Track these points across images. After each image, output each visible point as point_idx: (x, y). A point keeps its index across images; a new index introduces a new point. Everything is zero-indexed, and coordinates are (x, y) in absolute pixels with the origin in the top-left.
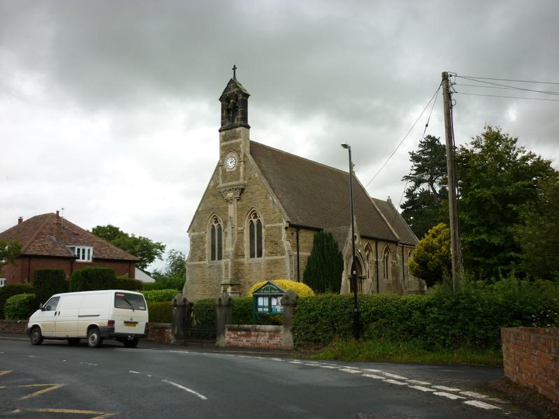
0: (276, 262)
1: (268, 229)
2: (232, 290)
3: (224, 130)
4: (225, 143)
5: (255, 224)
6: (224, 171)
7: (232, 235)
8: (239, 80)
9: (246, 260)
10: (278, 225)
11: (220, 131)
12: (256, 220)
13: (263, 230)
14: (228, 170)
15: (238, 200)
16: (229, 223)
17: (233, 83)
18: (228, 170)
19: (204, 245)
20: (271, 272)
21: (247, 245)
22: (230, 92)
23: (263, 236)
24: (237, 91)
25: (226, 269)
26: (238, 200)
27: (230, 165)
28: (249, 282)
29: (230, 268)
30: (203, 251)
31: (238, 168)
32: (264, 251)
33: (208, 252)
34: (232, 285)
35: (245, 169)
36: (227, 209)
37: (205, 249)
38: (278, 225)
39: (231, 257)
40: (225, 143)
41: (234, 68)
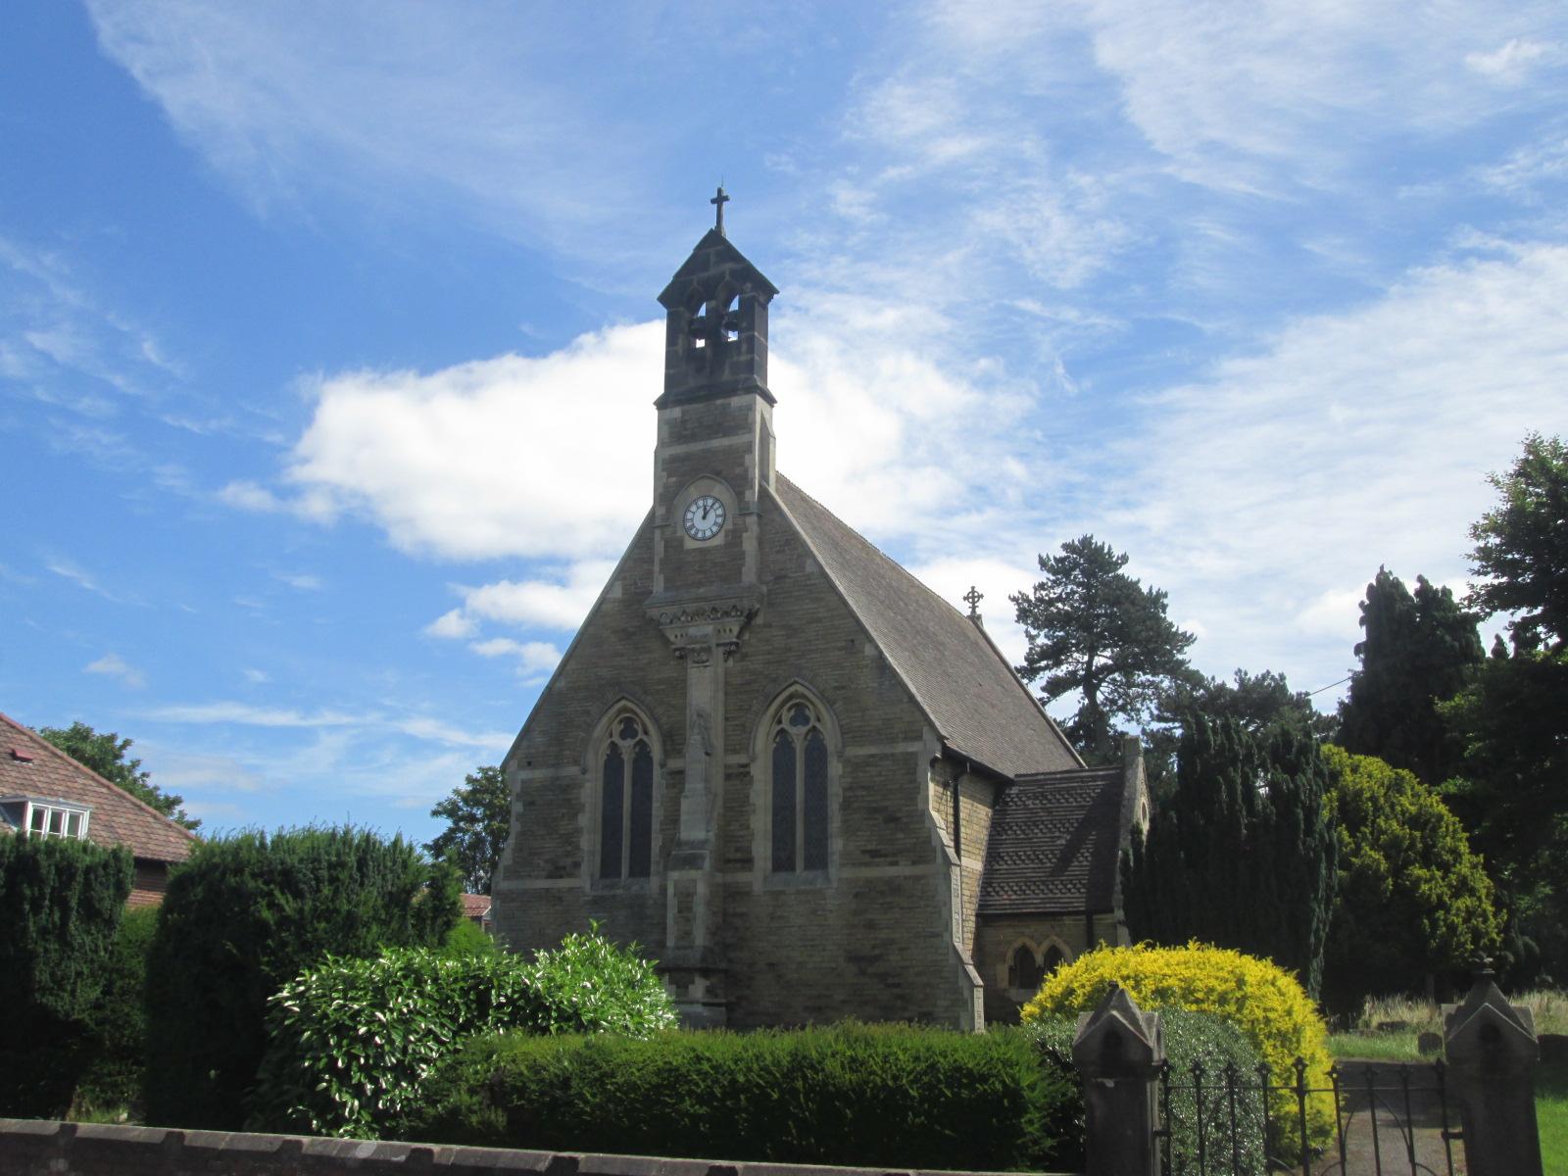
0: (893, 887)
1: (855, 766)
2: (709, 991)
3: (678, 402)
4: (679, 450)
5: (799, 746)
6: (674, 546)
7: (707, 780)
8: (730, 234)
9: (758, 877)
10: (901, 748)
11: (661, 404)
12: (804, 729)
13: (835, 769)
14: (690, 544)
15: (729, 654)
16: (694, 739)
17: (714, 245)
18: (690, 544)
19: (574, 816)
20: (871, 926)
21: (761, 822)
22: (704, 275)
23: (835, 791)
24: (733, 273)
25: (685, 908)
26: (729, 654)
27: (699, 523)
28: (771, 965)
29: (700, 909)
30: (570, 839)
31: (734, 537)
32: (836, 845)
33: (589, 842)
34: (705, 973)
35: (761, 542)
36: (680, 686)
37: (578, 831)
38: (901, 748)
39: (707, 864)
40: (679, 450)
41: (720, 200)
